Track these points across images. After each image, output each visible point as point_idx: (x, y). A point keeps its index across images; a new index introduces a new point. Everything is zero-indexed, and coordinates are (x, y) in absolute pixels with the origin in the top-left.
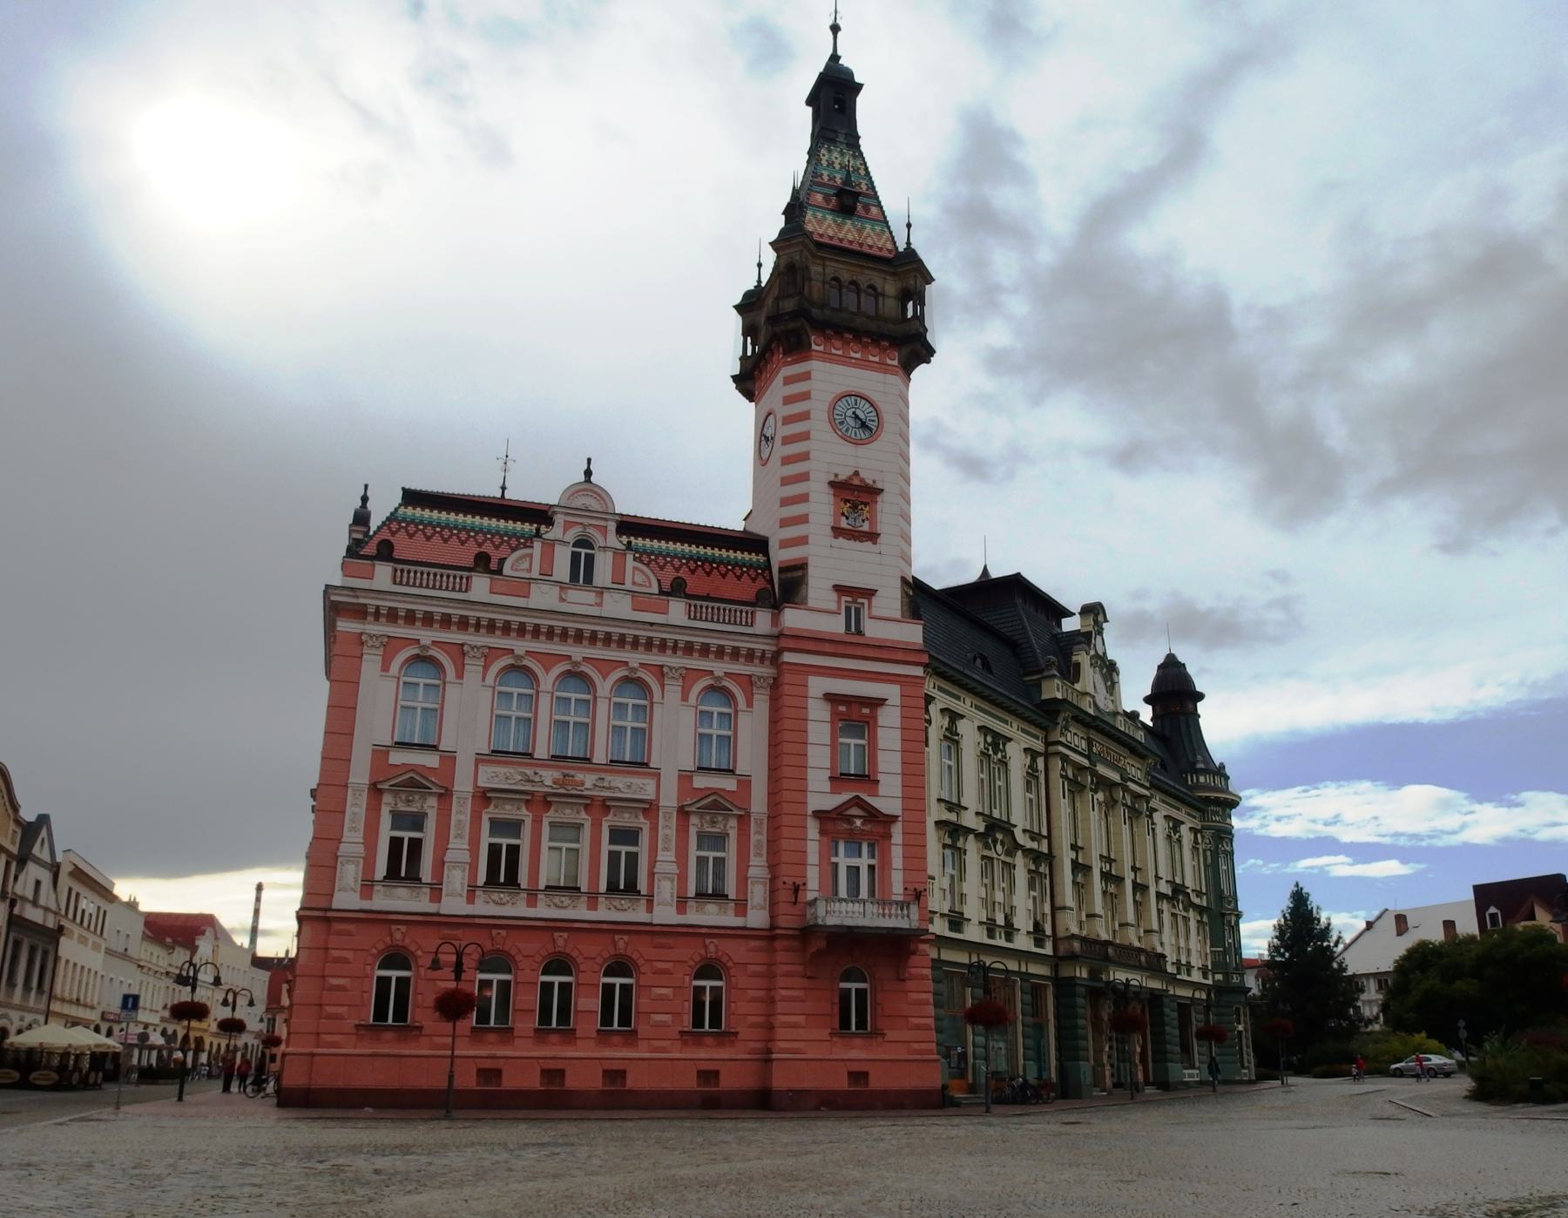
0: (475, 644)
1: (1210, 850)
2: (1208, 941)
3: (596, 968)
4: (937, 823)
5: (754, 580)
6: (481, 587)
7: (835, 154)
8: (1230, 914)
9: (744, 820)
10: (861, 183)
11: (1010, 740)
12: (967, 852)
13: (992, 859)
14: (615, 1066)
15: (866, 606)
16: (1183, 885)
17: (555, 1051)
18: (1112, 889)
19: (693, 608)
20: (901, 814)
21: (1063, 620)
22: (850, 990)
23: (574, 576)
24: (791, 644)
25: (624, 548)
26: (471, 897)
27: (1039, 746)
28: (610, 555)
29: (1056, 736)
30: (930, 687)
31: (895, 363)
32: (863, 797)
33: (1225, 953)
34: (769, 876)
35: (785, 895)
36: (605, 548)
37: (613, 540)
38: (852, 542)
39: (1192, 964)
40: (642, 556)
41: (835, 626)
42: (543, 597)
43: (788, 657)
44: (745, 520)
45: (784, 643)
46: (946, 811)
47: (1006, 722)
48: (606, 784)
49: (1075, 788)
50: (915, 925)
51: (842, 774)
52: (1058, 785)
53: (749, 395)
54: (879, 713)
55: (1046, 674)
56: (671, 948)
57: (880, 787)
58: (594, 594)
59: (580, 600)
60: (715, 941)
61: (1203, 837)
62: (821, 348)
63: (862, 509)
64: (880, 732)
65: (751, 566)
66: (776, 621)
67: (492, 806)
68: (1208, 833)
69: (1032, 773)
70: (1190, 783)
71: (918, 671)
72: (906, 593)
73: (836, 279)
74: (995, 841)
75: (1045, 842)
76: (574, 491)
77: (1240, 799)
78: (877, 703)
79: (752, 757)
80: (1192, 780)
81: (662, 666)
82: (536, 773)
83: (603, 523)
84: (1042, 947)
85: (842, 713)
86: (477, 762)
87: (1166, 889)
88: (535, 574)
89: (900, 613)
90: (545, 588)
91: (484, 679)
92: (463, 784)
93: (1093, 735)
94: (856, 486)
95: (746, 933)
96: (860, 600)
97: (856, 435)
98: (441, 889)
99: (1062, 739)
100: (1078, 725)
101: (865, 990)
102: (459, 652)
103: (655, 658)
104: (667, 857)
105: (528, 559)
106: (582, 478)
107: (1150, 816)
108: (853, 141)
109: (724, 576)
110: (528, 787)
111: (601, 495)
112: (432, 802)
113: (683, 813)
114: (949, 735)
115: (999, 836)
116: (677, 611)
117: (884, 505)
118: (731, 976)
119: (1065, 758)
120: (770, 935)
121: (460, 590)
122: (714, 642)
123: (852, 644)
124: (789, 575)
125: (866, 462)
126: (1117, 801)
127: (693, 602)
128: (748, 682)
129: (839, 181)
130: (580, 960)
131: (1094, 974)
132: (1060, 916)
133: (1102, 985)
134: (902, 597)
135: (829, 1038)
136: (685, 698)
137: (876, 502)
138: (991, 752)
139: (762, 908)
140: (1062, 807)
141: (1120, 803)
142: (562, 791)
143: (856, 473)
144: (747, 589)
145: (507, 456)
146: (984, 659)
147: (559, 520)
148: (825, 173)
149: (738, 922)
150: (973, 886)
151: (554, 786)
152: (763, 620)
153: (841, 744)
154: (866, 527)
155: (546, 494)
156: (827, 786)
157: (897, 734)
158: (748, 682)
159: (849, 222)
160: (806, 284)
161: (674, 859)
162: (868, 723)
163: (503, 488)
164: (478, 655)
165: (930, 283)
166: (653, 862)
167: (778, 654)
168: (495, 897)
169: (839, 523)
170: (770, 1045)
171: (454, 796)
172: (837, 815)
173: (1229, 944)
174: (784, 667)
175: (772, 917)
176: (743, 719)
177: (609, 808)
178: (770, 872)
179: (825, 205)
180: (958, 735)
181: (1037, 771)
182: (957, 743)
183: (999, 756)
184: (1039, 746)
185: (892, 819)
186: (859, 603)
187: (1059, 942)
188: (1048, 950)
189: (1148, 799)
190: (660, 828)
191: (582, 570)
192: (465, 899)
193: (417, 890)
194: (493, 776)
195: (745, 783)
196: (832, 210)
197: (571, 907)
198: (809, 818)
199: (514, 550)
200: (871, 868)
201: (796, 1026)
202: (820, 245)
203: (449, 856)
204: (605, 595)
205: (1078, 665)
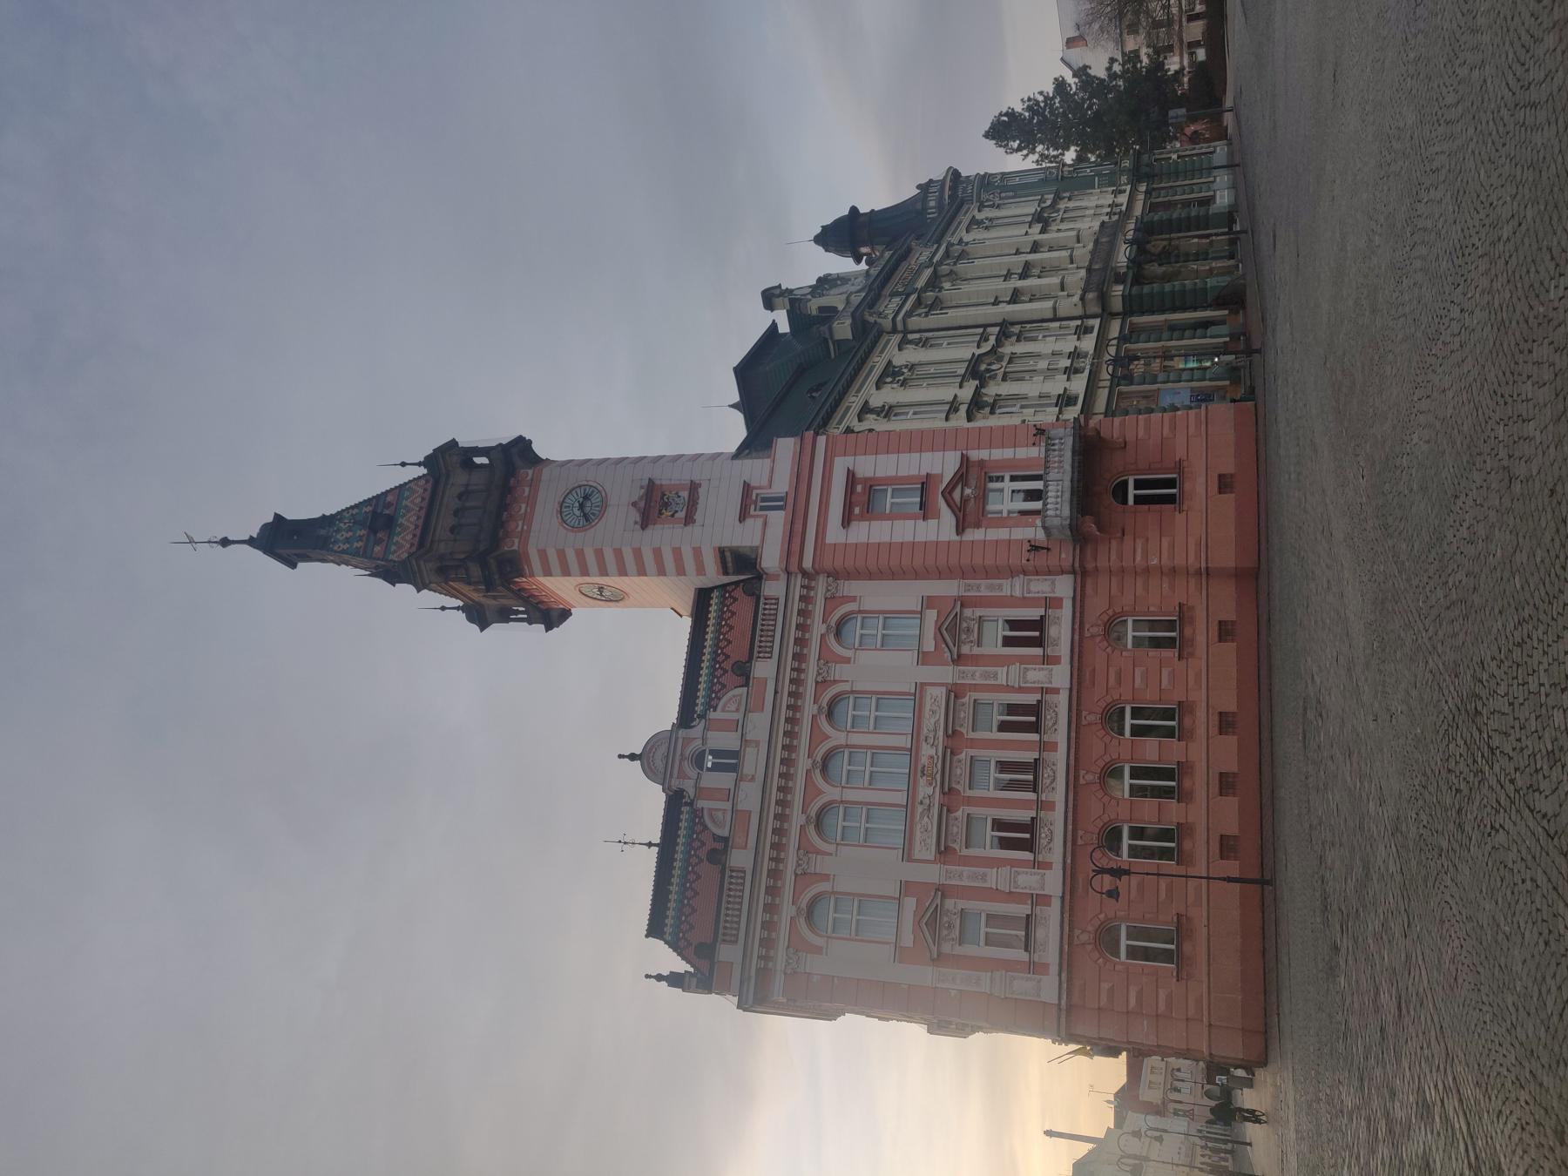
0: (795, 862)
1: (1000, 193)
2: (1091, 191)
3: (1115, 742)
4: (969, 420)
5: (735, 599)
6: (740, 858)
7: (338, 537)
8: (1062, 172)
9: (964, 602)
10: (365, 512)
11: (890, 362)
12: (999, 393)
13: (1005, 373)
14: (1215, 720)
15: (758, 491)
16: (1033, 215)
17: (1200, 783)
18: (1036, 271)
19: (761, 655)
20: (959, 454)
21: (780, 332)
22: (1136, 496)
23: (733, 768)
24: (794, 560)
25: (704, 720)
26: (1048, 866)
27: (896, 338)
28: (710, 734)
29: (887, 324)
30: (835, 430)
31: (530, 472)
32: (944, 486)
33: (1099, 175)
34: (1022, 576)
35: (1040, 559)
36: (704, 739)
37: (697, 730)
38: (699, 506)
39: (1111, 202)
40: (711, 705)
41: (778, 519)
42: (749, 797)
43: (808, 563)
44: (681, 616)
45: (794, 568)
46: (958, 413)
47: (873, 367)
48: (931, 735)
49: (937, 304)
50: (1069, 431)
51: (921, 509)
52: (935, 320)
53: (565, 614)
54: (862, 476)
55: (827, 336)
56: (1094, 670)
57: (933, 472)
58: (747, 749)
59: (753, 762)
60: (1087, 626)
61: (987, 201)
62: (516, 541)
63: (668, 499)
64: (879, 474)
65: (722, 604)
66: (776, 577)
67: (954, 846)
68: (984, 196)
69: (924, 344)
70: (936, 215)
71: (822, 440)
72: (748, 454)
73: (452, 530)
74: (988, 371)
75: (989, 330)
76: (650, 772)
77: (951, 167)
78: (851, 478)
79: (904, 595)
80: (934, 213)
81: (817, 683)
82: (921, 803)
83: (680, 741)
84: (1093, 327)
85: (861, 511)
86: (910, 860)
87: (1037, 227)
88: (727, 806)
89: (766, 460)
90: (741, 795)
91: (831, 854)
92: (933, 874)
93: (887, 291)
94: (646, 504)
95: (1078, 598)
96: (754, 498)
97: (598, 506)
98: (1037, 895)
99: (891, 317)
100: (878, 304)
101: (1136, 480)
102: (803, 877)
103: (809, 689)
104: (1002, 675)
105: (713, 813)
106: (638, 763)
107: (967, 244)
108: (326, 520)
109: (731, 628)
110: (935, 811)
111: (653, 743)
112: (949, 904)
113: (959, 660)
114: (884, 413)
115: (983, 367)
116: (763, 669)
117: (664, 477)
118: (1122, 612)
119: (909, 314)
120: (1082, 574)
121: (743, 878)
122: (793, 633)
123: (795, 505)
124: (730, 565)
125: (622, 496)
126: (951, 271)
127: (756, 654)
128: (832, 600)
129: (363, 532)
130: (1107, 759)
131: (1120, 279)
132: (1061, 313)
133: (1130, 274)
134: (751, 458)
135: (1185, 513)
136: (847, 661)
137: (661, 485)
138: (901, 378)
139: (1053, 583)
140: (953, 316)
141: (954, 268)
142: (938, 777)
143: (634, 504)
144: (744, 606)
145: (620, 842)
146: (811, 391)
147: (675, 784)
148: (356, 545)
149: (1068, 605)
150: (1031, 388)
151: (934, 784)
152: (774, 589)
153: (891, 511)
154: (685, 494)
155: (654, 799)
156: (932, 523)
157: (882, 458)
158: (832, 600)
159: (400, 520)
160: (457, 556)
161: (1005, 669)
162: (871, 486)
163: (650, 845)
164: (805, 859)
165: (457, 443)
166: (1008, 688)
167: (805, 574)
168: (1044, 842)
169: (681, 519)
170: (1191, 570)
171: (945, 883)
172: (960, 511)
173: (1091, 171)
174: (817, 566)
175: (1063, 572)
176: (868, 604)
177: (954, 732)
178: (1018, 575)
179: (385, 543)
180: (884, 406)
181: (920, 339)
182: (891, 407)
183: (905, 370)
184: (896, 338)
185: (965, 460)
186: (757, 497)
187: (1088, 313)
188: (1096, 323)
189: (950, 245)
190: (974, 682)
191: (729, 761)
192: (1047, 872)
193: (1039, 918)
194: (925, 847)
195: (929, 602)
196: (389, 538)
197: (1054, 768)
198: (964, 539)
199: (706, 827)
200: (1013, 479)
201: (1172, 546)
202: (421, 545)
203: (1005, 888)
204: (748, 739)
205: (821, 309)
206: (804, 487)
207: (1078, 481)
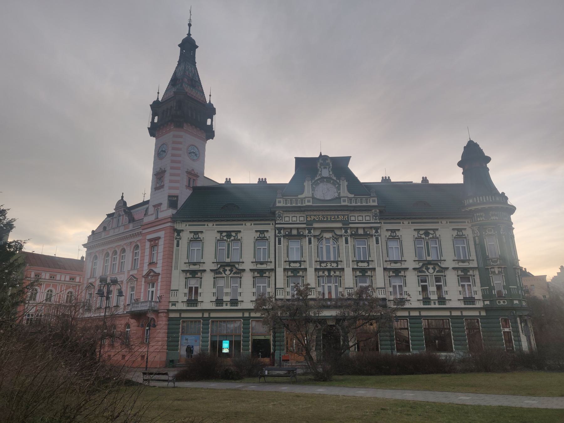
20: (160, 272)
30: (179, 226)
185: (159, 274)
206: (163, 222)
207: (134, 313)
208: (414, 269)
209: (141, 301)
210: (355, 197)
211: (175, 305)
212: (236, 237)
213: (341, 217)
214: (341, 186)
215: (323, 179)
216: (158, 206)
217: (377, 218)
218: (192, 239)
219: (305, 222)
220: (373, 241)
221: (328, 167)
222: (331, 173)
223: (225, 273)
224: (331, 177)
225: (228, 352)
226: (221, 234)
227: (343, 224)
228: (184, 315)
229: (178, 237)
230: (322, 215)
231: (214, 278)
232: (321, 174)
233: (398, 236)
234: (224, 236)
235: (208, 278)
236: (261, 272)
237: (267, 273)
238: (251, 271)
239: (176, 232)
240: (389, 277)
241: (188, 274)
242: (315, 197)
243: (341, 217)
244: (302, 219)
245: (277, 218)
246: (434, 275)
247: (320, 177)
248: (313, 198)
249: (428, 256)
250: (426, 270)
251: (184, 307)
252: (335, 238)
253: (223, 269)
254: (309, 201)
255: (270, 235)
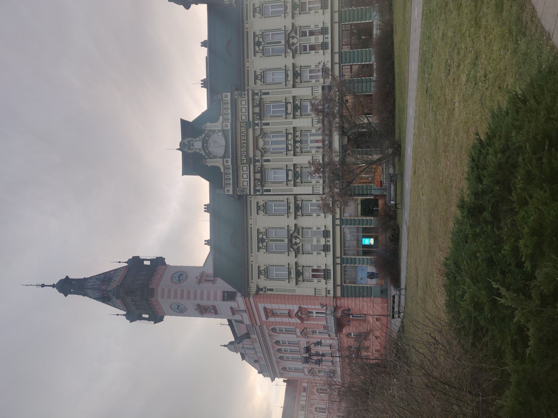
20: (298, 306)
30: (253, 289)
185: (300, 308)
208: (293, 57)
209: (325, 323)
210: (222, 115)
211: (329, 291)
212: (264, 233)
213: (243, 129)
214: (211, 129)
215: (204, 147)
216: (233, 311)
217: (243, 93)
218: (266, 276)
219: (248, 165)
220: (267, 98)
221: (192, 142)
222: (198, 139)
223: (298, 244)
224: (202, 139)
225: (373, 239)
226: (260, 248)
227: (250, 127)
228: (339, 282)
229: (264, 290)
230: (241, 148)
231: (303, 254)
232: (199, 149)
233: (261, 73)
234: (263, 245)
235: (304, 260)
236: (297, 208)
237: (298, 202)
238: (296, 219)
239: (259, 292)
240: (301, 82)
241: (300, 279)
242: (222, 155)
243: (243, 129)
244: (245, 169)
245: (245, 193)
246: (300, 37)
247: (202, 150)
248: (224, 157)
249: (281, 43)
250: (295, 46)
251: (331, 281)
252: (264, 135)
253: (294, 245)
254: (227, 162)
255: (261, 200)
